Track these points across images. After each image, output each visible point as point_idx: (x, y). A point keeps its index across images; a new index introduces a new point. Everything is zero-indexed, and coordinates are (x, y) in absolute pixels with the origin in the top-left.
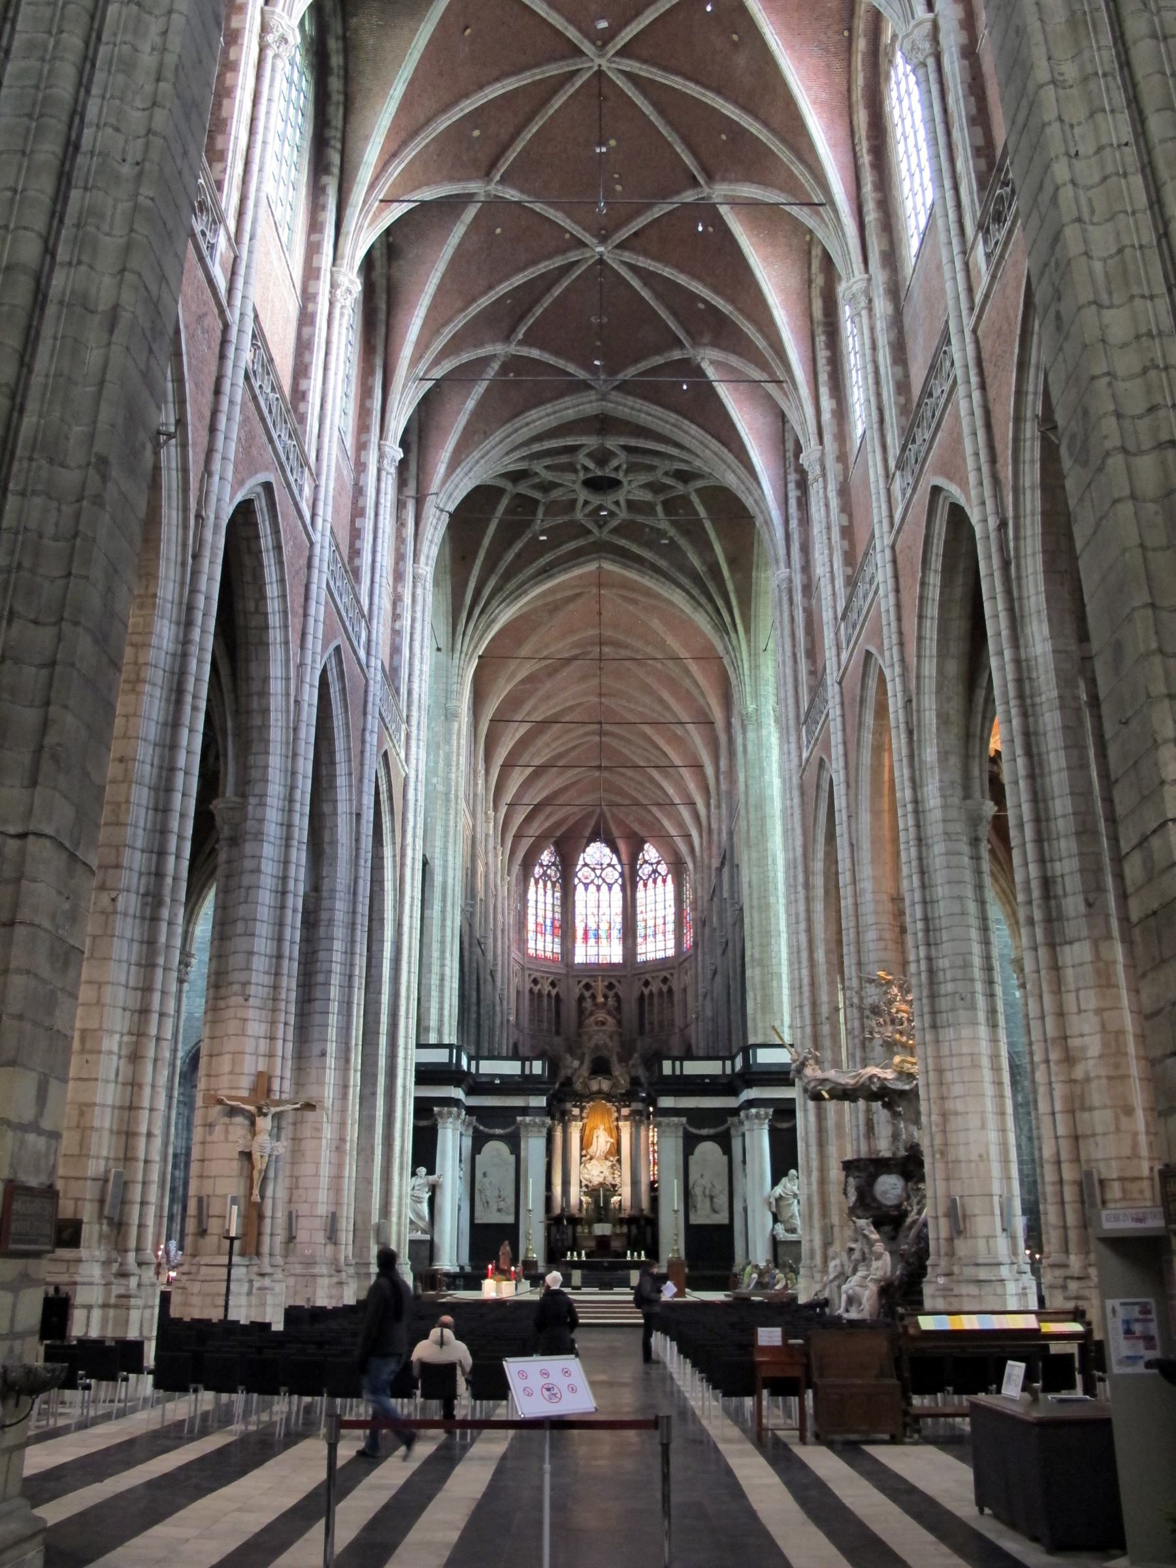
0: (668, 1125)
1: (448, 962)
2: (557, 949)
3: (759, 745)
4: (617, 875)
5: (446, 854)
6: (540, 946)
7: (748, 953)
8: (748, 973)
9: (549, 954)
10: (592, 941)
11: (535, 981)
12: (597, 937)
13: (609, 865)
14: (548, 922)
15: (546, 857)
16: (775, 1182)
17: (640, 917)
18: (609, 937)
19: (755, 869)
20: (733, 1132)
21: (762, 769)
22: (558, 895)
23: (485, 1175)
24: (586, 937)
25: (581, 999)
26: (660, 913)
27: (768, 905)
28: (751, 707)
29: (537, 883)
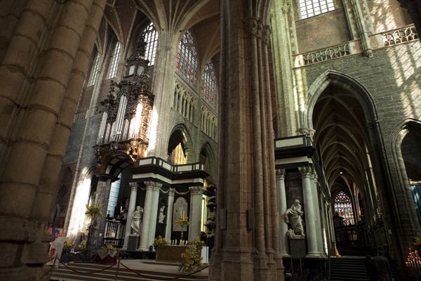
16: (288, 208)
23: (177, 211)
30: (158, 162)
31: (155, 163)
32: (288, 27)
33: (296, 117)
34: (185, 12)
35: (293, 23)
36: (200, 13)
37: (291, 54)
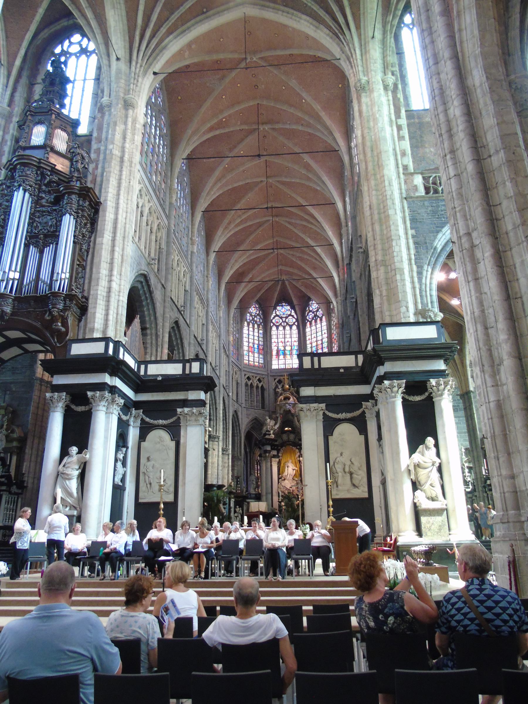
0: (309, 410)
1: (114, 278)
2: (262, 361)
3: (373, 105)
4: (294, 320)
5: (118, 199)
6: (251, 359)
7: (372, 259)
8: (374, 275)
9: (257, 364)
10: (281, 357)
11: (249, 378)
12: (285, 354)
13: (290, 315)
14: (256, 346)
15: (253, 310)
17: (308, 342)
18: (291, 354)
19: (374, 193)
20: (367, 415)
21: (375, 120)
22: (261, 332)
23: (148, 459)
24: (278, 355)
25: (277, 387)
26: (319, 338)
27: (388, 217)
28: (364, 79)
29: (248, 325)
30: (116, 351)
31: (111, 352)
32: (393, 118)
33: (414, 288)
34: (170, 32)
35: (403, 113)
36: (193, 46)
37: (401, 170)
